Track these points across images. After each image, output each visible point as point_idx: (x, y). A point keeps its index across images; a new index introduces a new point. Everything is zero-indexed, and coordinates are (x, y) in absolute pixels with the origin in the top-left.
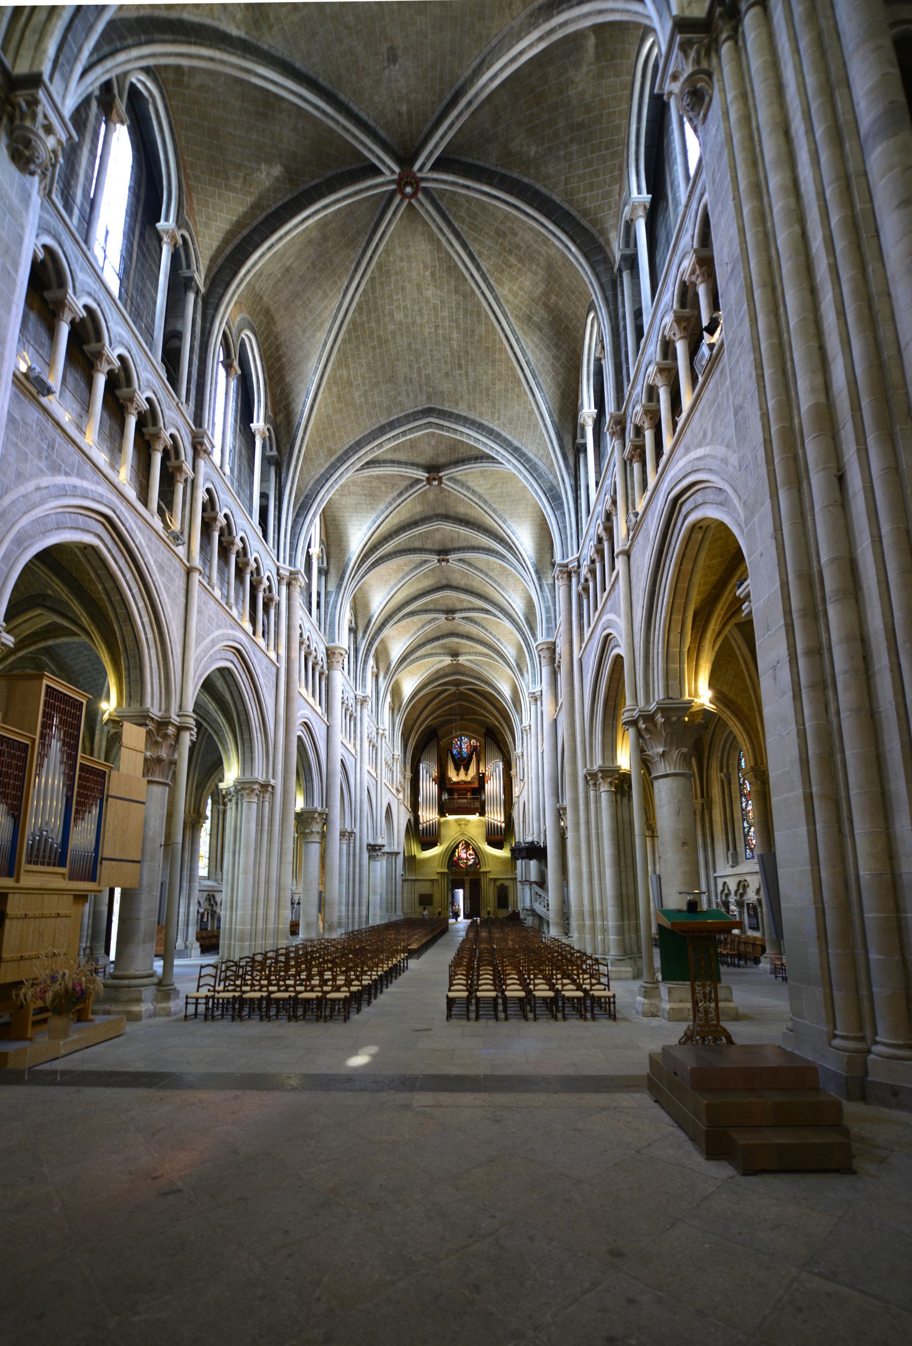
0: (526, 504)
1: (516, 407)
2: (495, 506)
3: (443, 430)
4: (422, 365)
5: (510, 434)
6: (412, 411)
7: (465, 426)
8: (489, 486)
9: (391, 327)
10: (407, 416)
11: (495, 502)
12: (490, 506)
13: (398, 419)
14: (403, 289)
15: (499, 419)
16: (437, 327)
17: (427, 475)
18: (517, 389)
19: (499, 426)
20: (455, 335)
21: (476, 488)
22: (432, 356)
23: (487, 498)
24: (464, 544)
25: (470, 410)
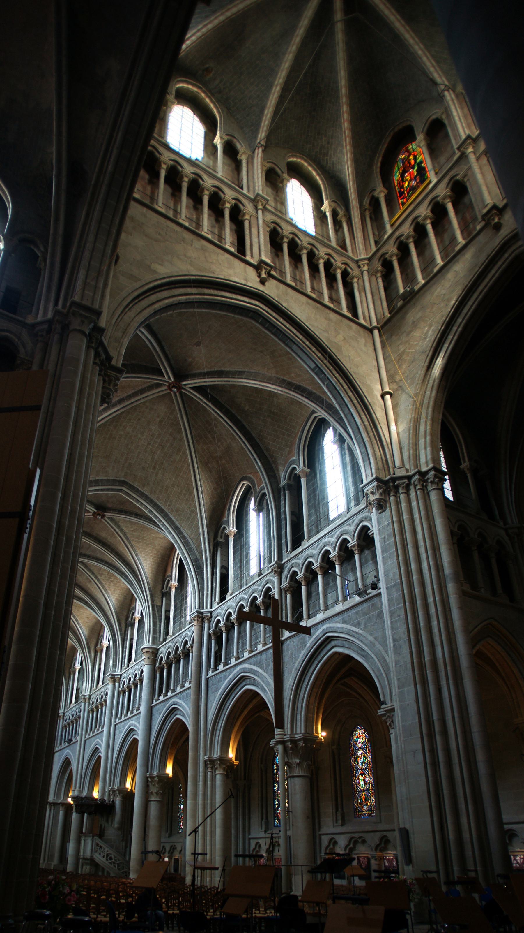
2: (133, 543)
3: (129, 497)
5: (174, 517)
6: (112, 478)
7: (145, 501)
11: (133, 540)
12: (130, 543)
13: (102, 480)
14: (139, 419)
15: (169, 506)
17: (96, 511)
19: (168, 510)
20: (159, 452)
21: (124, 528)
23: (129, 536)
25: (151, 492)
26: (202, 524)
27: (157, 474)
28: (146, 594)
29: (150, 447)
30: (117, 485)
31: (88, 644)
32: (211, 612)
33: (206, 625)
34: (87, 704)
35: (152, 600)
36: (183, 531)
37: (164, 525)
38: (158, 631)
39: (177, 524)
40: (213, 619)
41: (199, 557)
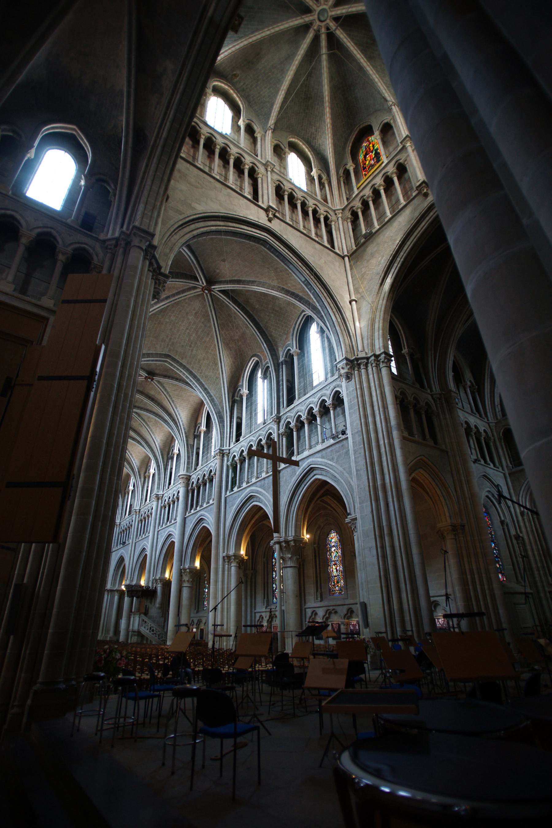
0: (188, 403)
1: (211, 373)
2: (173, 399)
3: (172, 366)
4: (173, 338)
8: (173, 389)
9: (168, 320)
10: (157, 354)
11: (174, 397)
12: (171, 399)
13: (152, 354)
15: (201, 373)
16: (187, 329)
17: (147, 375)
18: (214, 367)
20: (194, 335)
21: (167, 388)
22: (179, 337)
23: (171, 394)
24: (142, 406)
26: (224, 387)
27: (192, 351)
28: (183, 436)
29: (188, 331)
30: (163, 358)
31: (139, 472)
32: (229, 450)
33: (225, 459)
34: (137, 516)
35: (187, 441)
36: (210, 392)
37: (196, 387)
38: (191, 463)
39: (206, 386)
40: (230, 455)
41: (221, 410)
